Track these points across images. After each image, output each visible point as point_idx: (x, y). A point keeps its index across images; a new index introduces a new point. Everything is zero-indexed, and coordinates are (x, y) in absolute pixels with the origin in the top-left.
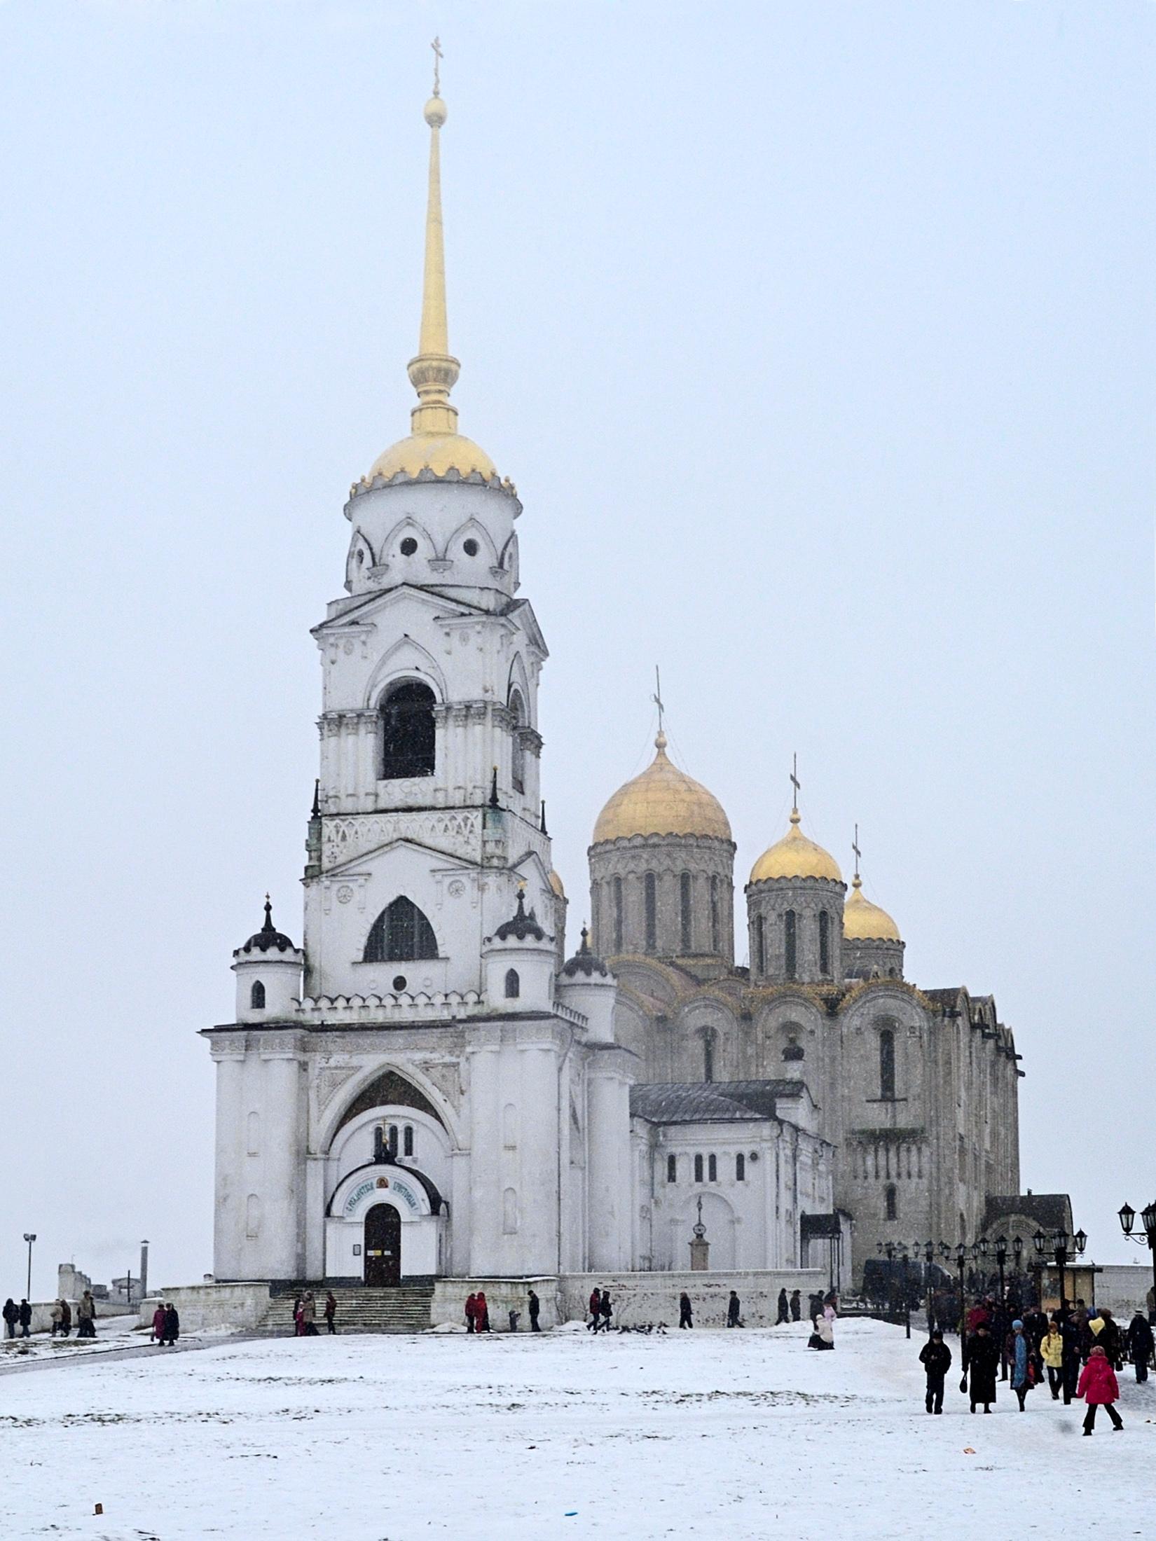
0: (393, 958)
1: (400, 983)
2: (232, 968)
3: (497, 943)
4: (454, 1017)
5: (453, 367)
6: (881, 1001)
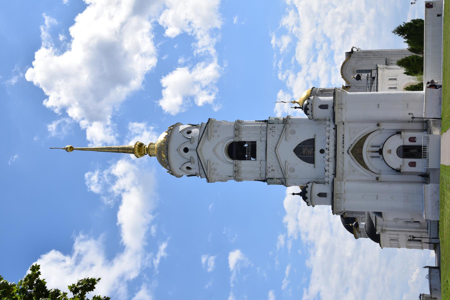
0: (314, 154)
1: (322, 151)
2: (314, 207)
3: (309, 112)
4: (334, 129)
5: (138, 144)
6: (347, 72)
